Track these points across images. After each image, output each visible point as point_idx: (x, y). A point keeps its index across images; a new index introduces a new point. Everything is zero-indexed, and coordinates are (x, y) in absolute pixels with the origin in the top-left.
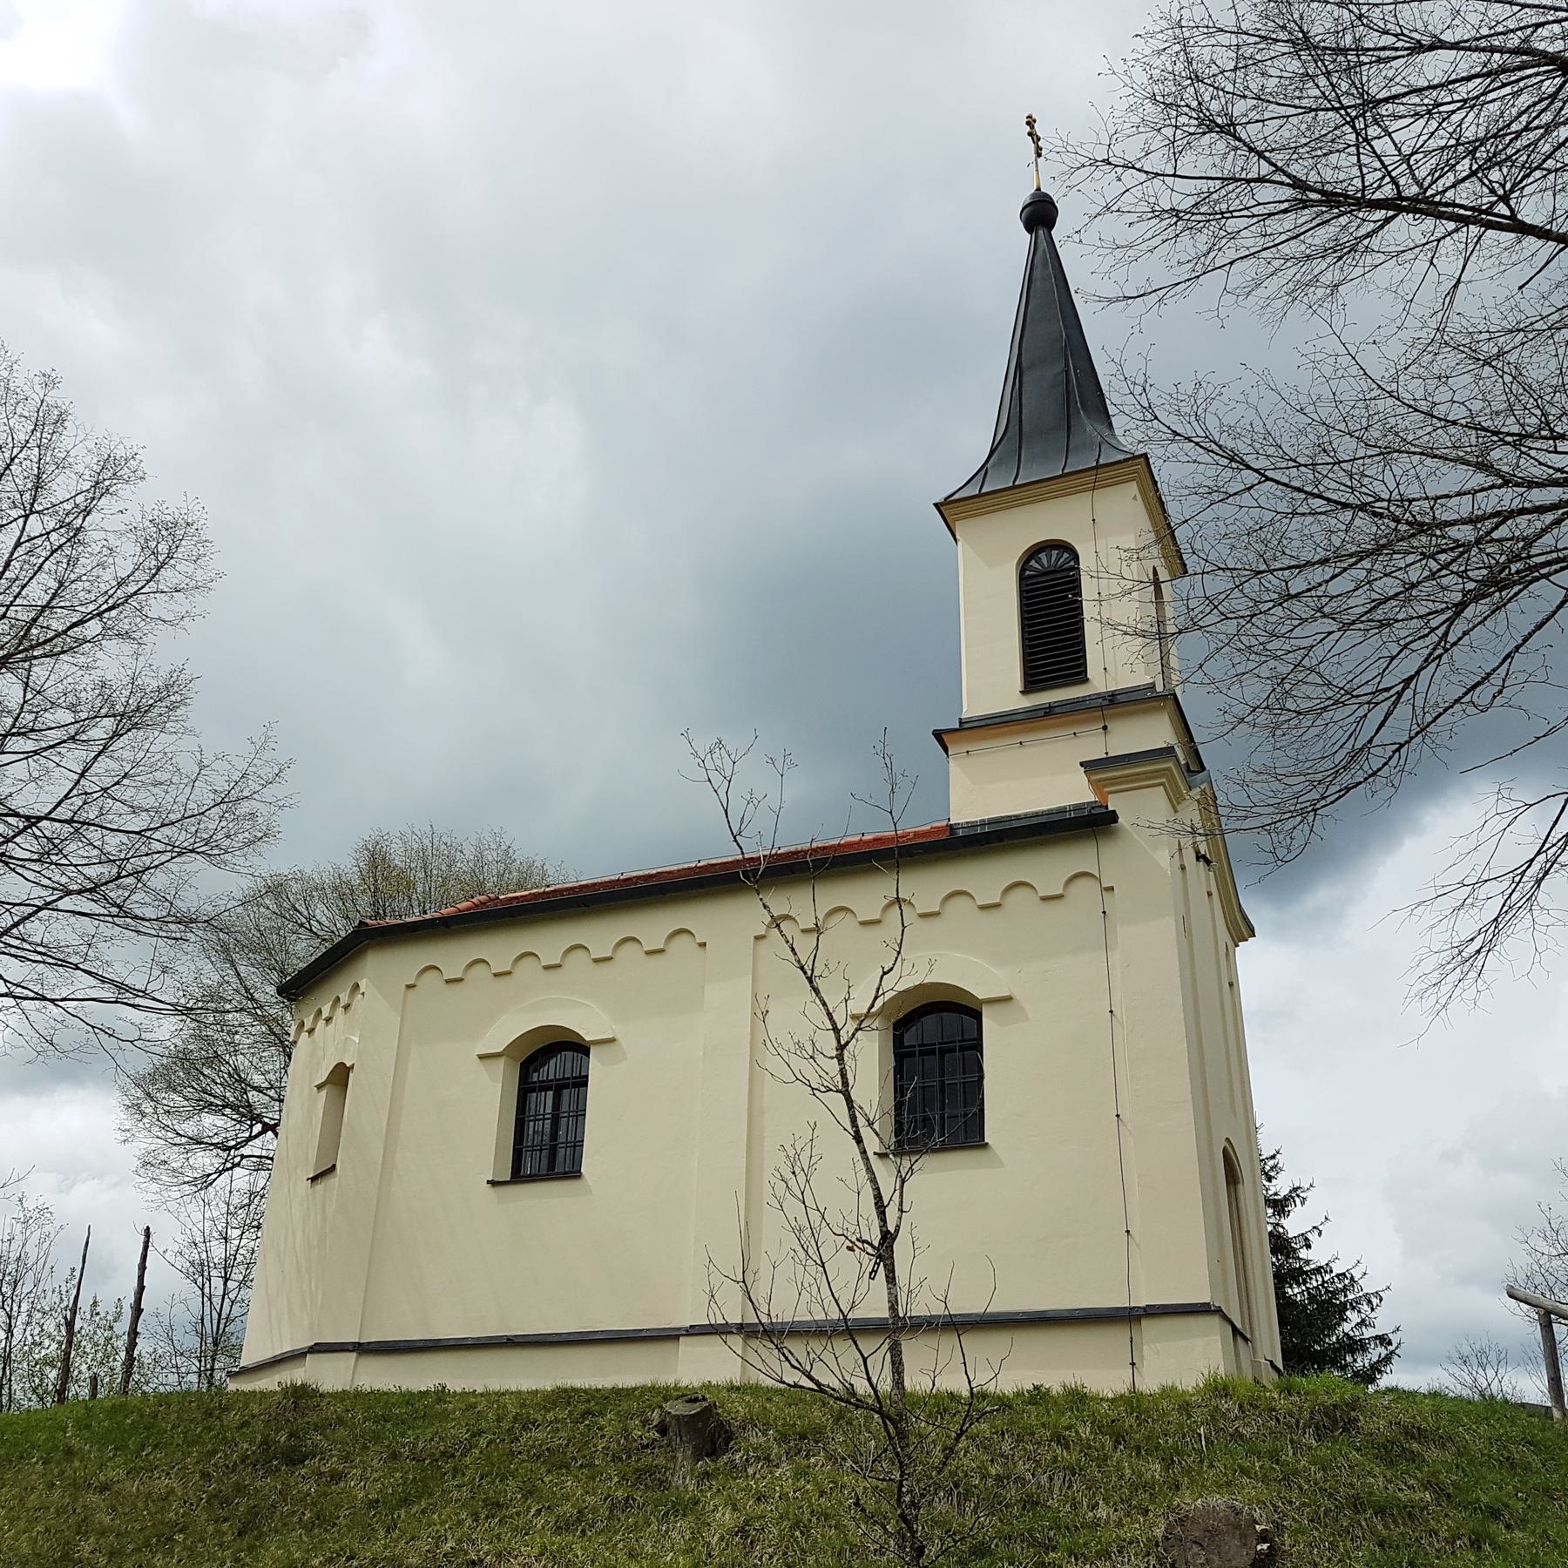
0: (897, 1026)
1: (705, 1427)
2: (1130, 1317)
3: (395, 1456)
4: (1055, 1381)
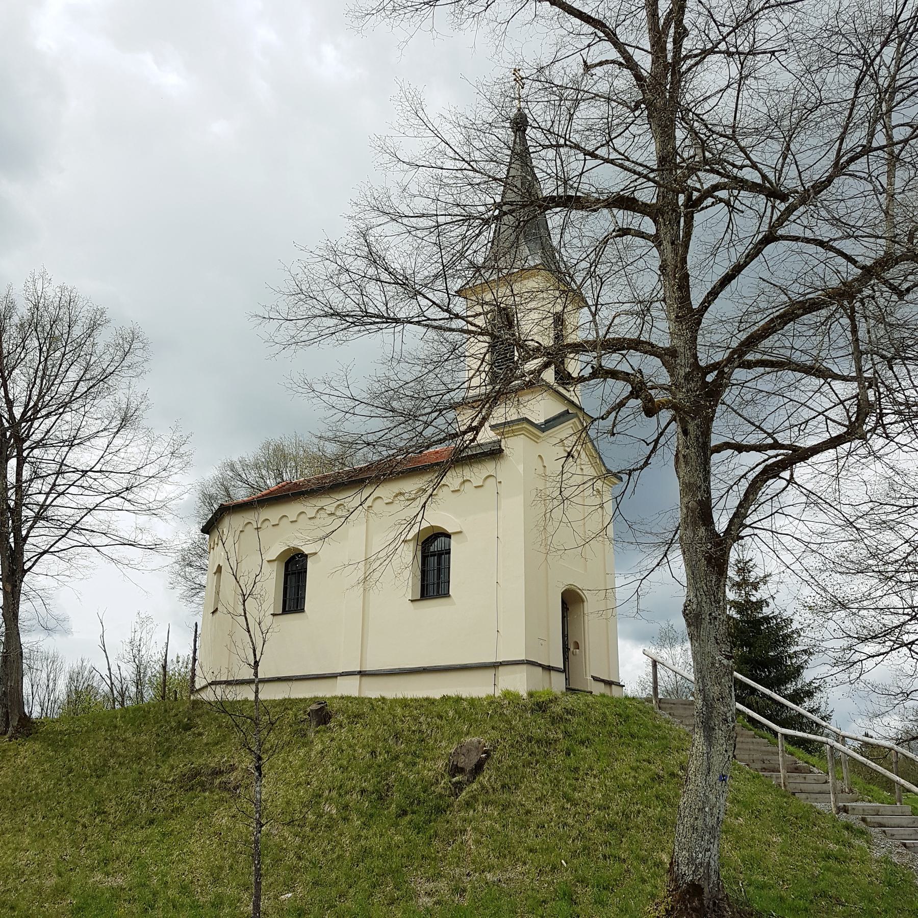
0: (287, 564)
1: (322, 714)
2: (495, 666)
3: (220, 726)
4: (452, 692)
